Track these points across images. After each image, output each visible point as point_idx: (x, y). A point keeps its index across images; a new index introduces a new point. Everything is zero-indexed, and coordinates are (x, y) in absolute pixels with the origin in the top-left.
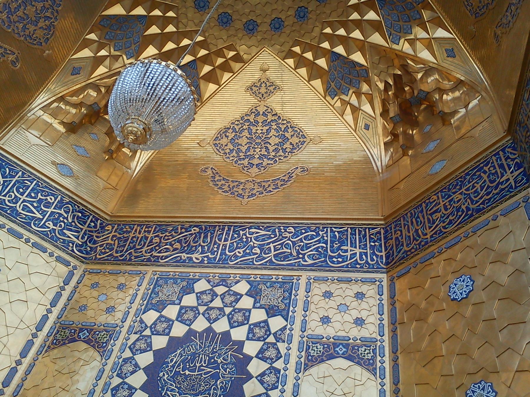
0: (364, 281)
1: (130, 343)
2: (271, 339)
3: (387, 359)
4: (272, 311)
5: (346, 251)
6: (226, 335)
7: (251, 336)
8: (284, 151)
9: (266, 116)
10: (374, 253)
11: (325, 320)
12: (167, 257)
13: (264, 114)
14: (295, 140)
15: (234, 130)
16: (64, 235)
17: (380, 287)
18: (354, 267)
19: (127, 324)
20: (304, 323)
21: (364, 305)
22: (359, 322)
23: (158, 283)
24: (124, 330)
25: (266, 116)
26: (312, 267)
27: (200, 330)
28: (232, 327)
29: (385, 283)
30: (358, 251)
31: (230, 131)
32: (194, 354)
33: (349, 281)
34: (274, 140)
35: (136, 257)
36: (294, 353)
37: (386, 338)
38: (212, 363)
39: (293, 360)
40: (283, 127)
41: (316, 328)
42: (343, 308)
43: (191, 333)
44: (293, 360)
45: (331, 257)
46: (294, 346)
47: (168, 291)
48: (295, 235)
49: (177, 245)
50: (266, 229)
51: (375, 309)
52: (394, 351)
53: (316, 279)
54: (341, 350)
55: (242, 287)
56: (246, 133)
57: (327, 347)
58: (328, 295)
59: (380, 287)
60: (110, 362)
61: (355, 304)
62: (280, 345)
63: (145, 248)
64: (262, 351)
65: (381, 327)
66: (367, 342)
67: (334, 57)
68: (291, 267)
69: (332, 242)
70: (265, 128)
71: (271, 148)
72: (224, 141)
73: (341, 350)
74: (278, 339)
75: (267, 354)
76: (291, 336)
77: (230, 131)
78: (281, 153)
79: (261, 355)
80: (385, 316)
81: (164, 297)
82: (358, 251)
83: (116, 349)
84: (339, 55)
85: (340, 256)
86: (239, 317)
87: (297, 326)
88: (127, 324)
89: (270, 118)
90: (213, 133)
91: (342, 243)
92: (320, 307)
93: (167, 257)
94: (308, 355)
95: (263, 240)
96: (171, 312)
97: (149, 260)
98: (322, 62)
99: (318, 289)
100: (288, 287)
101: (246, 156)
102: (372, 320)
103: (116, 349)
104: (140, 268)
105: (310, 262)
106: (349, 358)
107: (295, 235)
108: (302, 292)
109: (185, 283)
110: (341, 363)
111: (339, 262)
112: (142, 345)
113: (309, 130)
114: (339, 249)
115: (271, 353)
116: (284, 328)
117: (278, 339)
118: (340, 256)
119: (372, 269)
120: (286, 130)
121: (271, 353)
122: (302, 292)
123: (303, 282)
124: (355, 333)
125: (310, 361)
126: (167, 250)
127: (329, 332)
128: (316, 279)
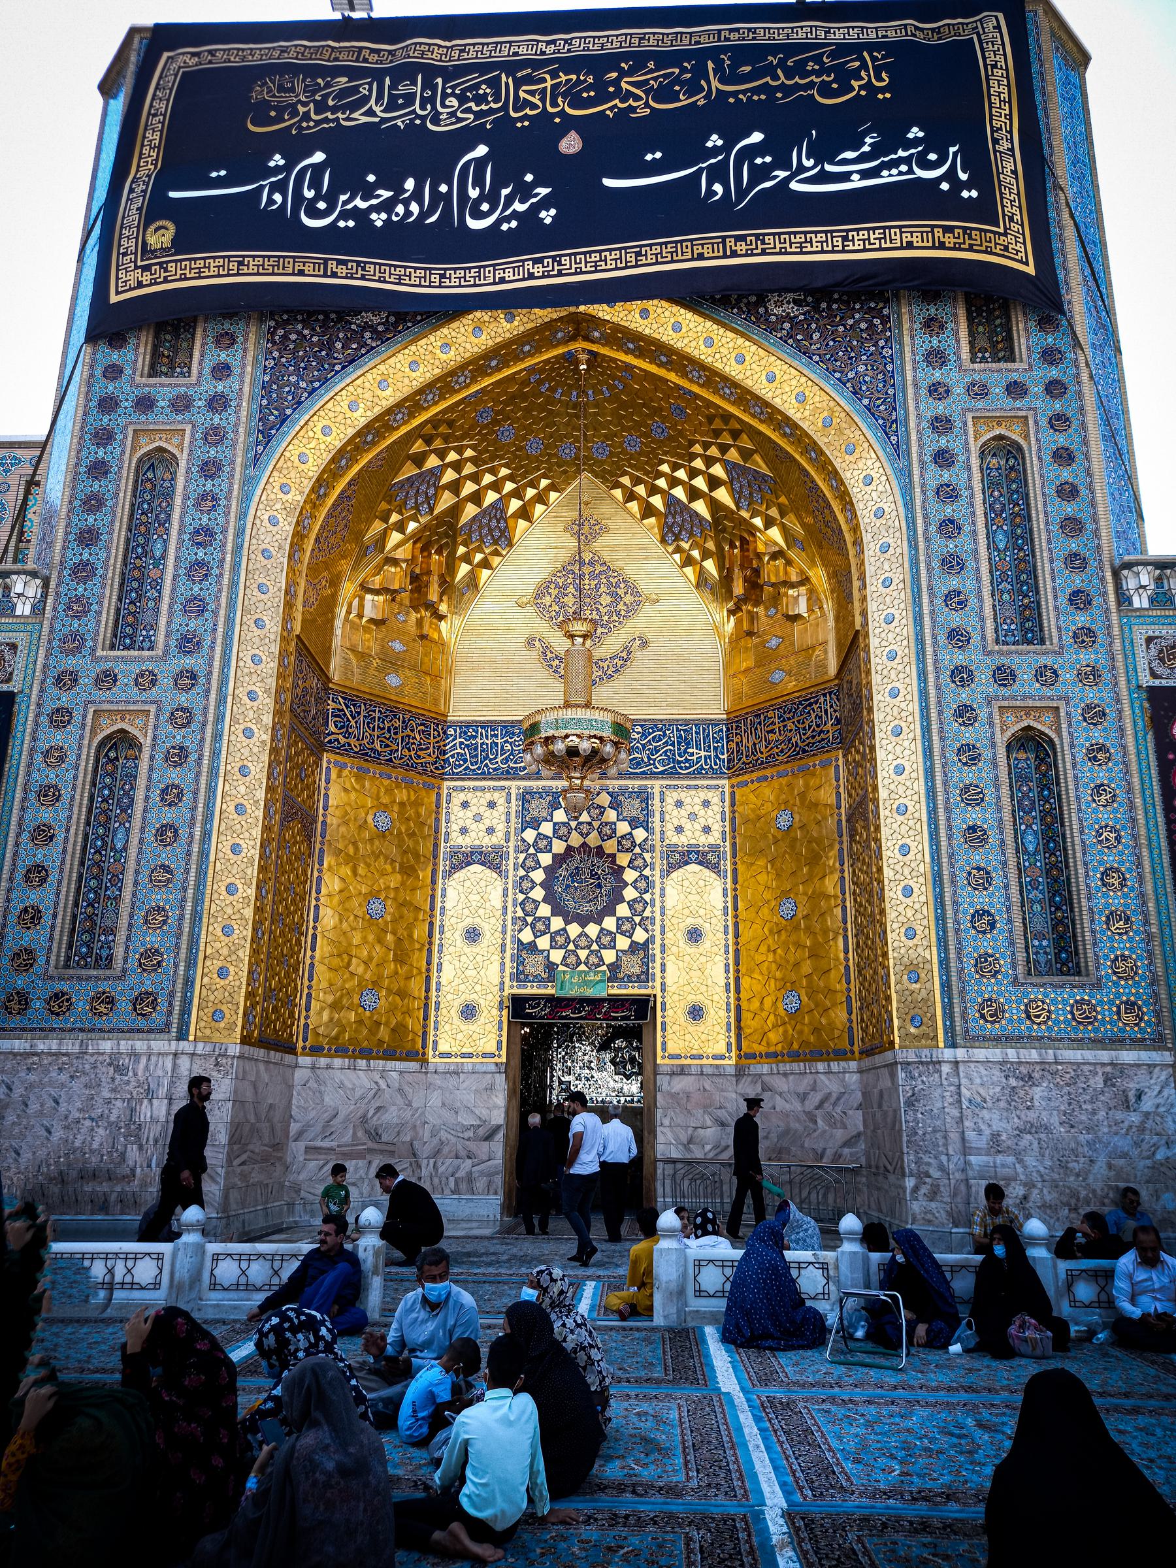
0: (709, 788)
2: (637, 850)
11: (679, 830)
13: (591, 563)
14: (628, 599)
18: (699, 774)
19: (511, 844)
20: (662, 833)
21: (710, 812)
22: (707, 830)
23: (526, 797)
24: (511, 850)
26: (663, 775)
29: (727, 790)
30: (703, 753)
33: (696, 788)
36: (658, 862)
38: (594, 875)
40: (614, 581)
41: (673, 838)
46: (657, 854)
47: (538, 807)
48: (644, 735)
51: (719, 817)
52: (734, 856)
53: (668, 787)
54: (693, 857)
55: (604, 799)
58: (679, 804)
59: (723, 793)
60: (510, 881)
61: (702, 813)
66: (714, 849)
67: (671, 502)
68: (644, 776)
69: (679, 743)
70: (594, 583)
71: (604, 611)
72: (547, 600)
73: (693, 857)
74: (643, 850)
75: (636, 863)
79: (631, 865)
82: (703, 753)
83: (511, 868)
84: (679, 501)
87: (657, 837)
88: (511, 844)
89: (598, 568)
90: (531, 589)
91: (688, 745)
96: (547, 828)
98: (657, 501)
100: (644, 796)
102: (716, 827)
103: (511, 868)
104: (502, 783)
106: (701, 863)
108: (657, 801)
110: (693, 867)
113: (644, 586)
114: (685, 752)
115: (639, 862)
118: (687, 760)
119: (717, 775)
121: (639, 862)
122: (657, 801)
123: (657, 791)
125: (672, 868)
127: (682, 840)
128: (668, 787)
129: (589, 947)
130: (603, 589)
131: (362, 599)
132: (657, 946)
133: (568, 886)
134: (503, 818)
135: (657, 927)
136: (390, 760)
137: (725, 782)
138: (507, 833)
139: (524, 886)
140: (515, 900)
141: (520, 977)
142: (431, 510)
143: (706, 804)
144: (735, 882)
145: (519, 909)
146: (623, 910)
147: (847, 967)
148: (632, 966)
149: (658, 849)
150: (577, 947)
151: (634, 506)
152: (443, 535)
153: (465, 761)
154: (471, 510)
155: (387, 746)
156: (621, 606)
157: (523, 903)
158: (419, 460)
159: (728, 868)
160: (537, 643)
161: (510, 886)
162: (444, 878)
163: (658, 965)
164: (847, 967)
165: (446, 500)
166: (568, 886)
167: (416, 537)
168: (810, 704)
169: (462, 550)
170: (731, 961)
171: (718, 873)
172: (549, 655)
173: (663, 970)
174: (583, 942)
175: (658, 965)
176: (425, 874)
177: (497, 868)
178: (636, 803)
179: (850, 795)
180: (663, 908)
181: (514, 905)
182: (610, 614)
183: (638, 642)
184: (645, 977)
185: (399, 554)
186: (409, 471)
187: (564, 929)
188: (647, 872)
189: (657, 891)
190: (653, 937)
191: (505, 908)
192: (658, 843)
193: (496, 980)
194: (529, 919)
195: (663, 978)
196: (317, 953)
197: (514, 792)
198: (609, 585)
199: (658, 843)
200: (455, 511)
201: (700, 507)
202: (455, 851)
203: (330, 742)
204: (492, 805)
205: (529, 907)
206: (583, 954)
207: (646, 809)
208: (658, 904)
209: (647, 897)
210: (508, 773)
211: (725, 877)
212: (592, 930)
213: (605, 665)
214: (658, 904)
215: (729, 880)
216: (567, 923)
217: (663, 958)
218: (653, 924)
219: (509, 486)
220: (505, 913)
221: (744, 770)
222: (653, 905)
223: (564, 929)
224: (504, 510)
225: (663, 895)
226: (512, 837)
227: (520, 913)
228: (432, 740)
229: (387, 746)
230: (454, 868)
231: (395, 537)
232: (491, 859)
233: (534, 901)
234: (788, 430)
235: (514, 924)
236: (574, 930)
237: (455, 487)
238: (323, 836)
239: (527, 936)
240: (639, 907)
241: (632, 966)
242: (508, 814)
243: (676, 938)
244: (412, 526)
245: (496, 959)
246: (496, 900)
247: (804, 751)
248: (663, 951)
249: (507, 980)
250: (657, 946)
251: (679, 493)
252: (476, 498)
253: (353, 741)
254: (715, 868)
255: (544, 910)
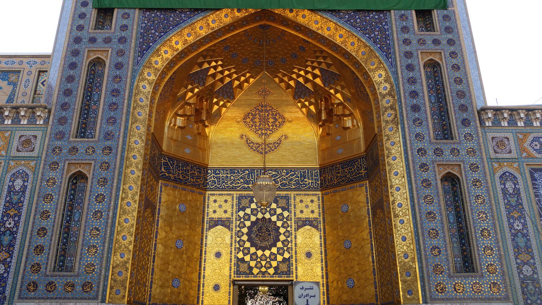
1: (238, 224)
2: (285, 220)
3: (322, 225)
4: (284, 209)
5: (306, 181)
6: (270, 219)
7: (278, 219)
8: (276, 126)
9: (266, 107)
10: (316, 182)
12: (239, 186)
15: (252, 114)
16: (197, 182)
17: (319, 197)
18: (309, 189)
19: (234, 217)
20: (295, 213)
22: (313, 212)
23: (240, 198)
24: (234, 220)
25: (266, 107)
27: (260, 218)
28: (271, 216)
29: (320, 196)
30: (310, 181)
31: (250, 115)
32: (261, 227)
34: (271, 120)
35: (227, 187)
36: (293, 225)
37: (321, 217)
39: (293, 227)
41: (299, 215)
42: (307, 206)
43: (258, 219)
44: (293, 227)
45: (301, 185)
46: (293, 222)
47: (244, 202)
48: (287, 174)
49: (242, 180)
50: (275, 171)
52: (324, 222)
54: (307, 223)
56: (258, 116)
57: (303, 222)
58: (301, 201)
61: (311, 204)
62: (288, 222)
63: (229, 183)
64: (283, 224)
65: (319, 213)
66: (316, 219)
67: (297, 83)
68: (287, 190)
69: (301, 177)
72: (248, 120)
73: (307, 223)
74: (287, 220)
75: (285, 225)
76: (291, 218)
77: (250, 115)
78: (275, 127)
79: (283, 226)
80: (321, 209)
81: (244, 205)
82: (310, 181)
83: (234, 227)
85: (304, 184)
86: (272, 212)
87: (293, 214)
88: (234, 217)
91: (305, 178)
92: (300, 206)
93: (239, 186)
94: (298, 225)
95: (275, 177)
96: (248, 211)
97: (232, 188)
98: (292, 83)
99: (298, 199)
100: (287, 198)
101: (260, 129)
102: (316, 211)
103: (234, 227)
105: (294, 187)
107: (287, 174)
109: (249, 199)
110: (308, 227)
111: (304, 187)
112: (242, 225)
114: (303, 180)
115: (286, 225)
116: (289, 215)
117: (287, 220)
118: (304, 184)
119: (316, 189)
120: (276, 115)
121: (286, 225)
123: (292, 196)
124: (311, 216)
125: (298, 227)
126: (239, 183)
127: (303, 216)
128: (297, 195)
129: (266, 260)
130: (270, 116)
131: (176, 119)
132: (294, 259)
133: (257, 234)
134: (231, 206)
135: (294, 252)
136: (186, 183)
137: (319, 193)
138: (232, 213)
139: (239, 234)
140: (235, 240)
141: (238, 272)
142: (204, 84)
143: (312, 201)
144: (325, 233)
145: (237, 244)
146: (279, 244)
147: (374, 269)
148: (284, 268)
149: (293, 220)
150: (261, 260)
151: (283, 85)
152: (207, 94)
153: (215, 183)
154: (220, 85)
155: (185, 177)
156: (277, 123)
157: (239, 242)
158: (201, 65)
159: (322, 227)
160: (244, 137)
161: (234, 234)
162: (206, 231)
163: (294, 267)
164: (374, 269)
165: (210, 81)
166: (257, 234)
167: (198, 94)
168: (354, 162)
169: (215, 100)
170: (324, 266)
171: (318, 229)
172: (249, 142)
173: (296, 270)
174: (263, 258)
175: (294, 267)
176: (199, 230)
177: (228, 227)
178: (285, 201)
179: (373, 198)
180: (296, 244)
181: (235, 243)
182: (272, 126)
183: (284, 137)
184: (289, 272)
185: (191, 101)
186: (197, 69)
187: (256, 253)
188: (289, 229)
189: (293, 237)
190: (292, 255)
191: (231, 244)
192: (293, 217)
193: (228, 274)
194: (242, 248)
195: (296, 273)
196: (155, 263)
197: (235, 196)
198: (273, 114)
199: (293, 217)
200: (213, 85)
201: (309, 86)
202: (212, 219)
203: (162, 175)
204: (226, 201)
205: (242, 243)
206: (264, 263)
207: (288, 204)
208: (294, 242)
209: (289, 239)
210: (232, 188)
211: (321, 231)
212: (267, 253)
213: (271, 146)
214: (294, 242)
215: (322, 232)
216: (257, 250)
217: (296, 265)
218: (292, 250)
219: (235, 76)
220: (231, 246)
221: (327, 188)
222: (292, 243)
223: (256, 253)
224: (232, 85)
225: (295, 238)
226: (234, 215)
227: (238, 246)
228: (202, 175)
229: (185, 177)
230: (211, 227)
231: (190, 94)
232: (225, 223)
233: (243, 241)
234: (347, 56)
235: (235, 250)
236: (260, 253)
237: (214, 76)
238: (159, 214)
239: (240, 255)
240: (286, 243)
241: (284, 268)
242: (233, 205)
243: (301, 256)
244: (196, 90)
245: (228, 265)
246: (228, 240)
247: (353, 181)
248: (296, 262)
249: (232, 274)
250: (294, 259)
251: (301, 80)
252: (222, 80)
253: (171, 175)
254: (316, 227)
255: (248, 245)
